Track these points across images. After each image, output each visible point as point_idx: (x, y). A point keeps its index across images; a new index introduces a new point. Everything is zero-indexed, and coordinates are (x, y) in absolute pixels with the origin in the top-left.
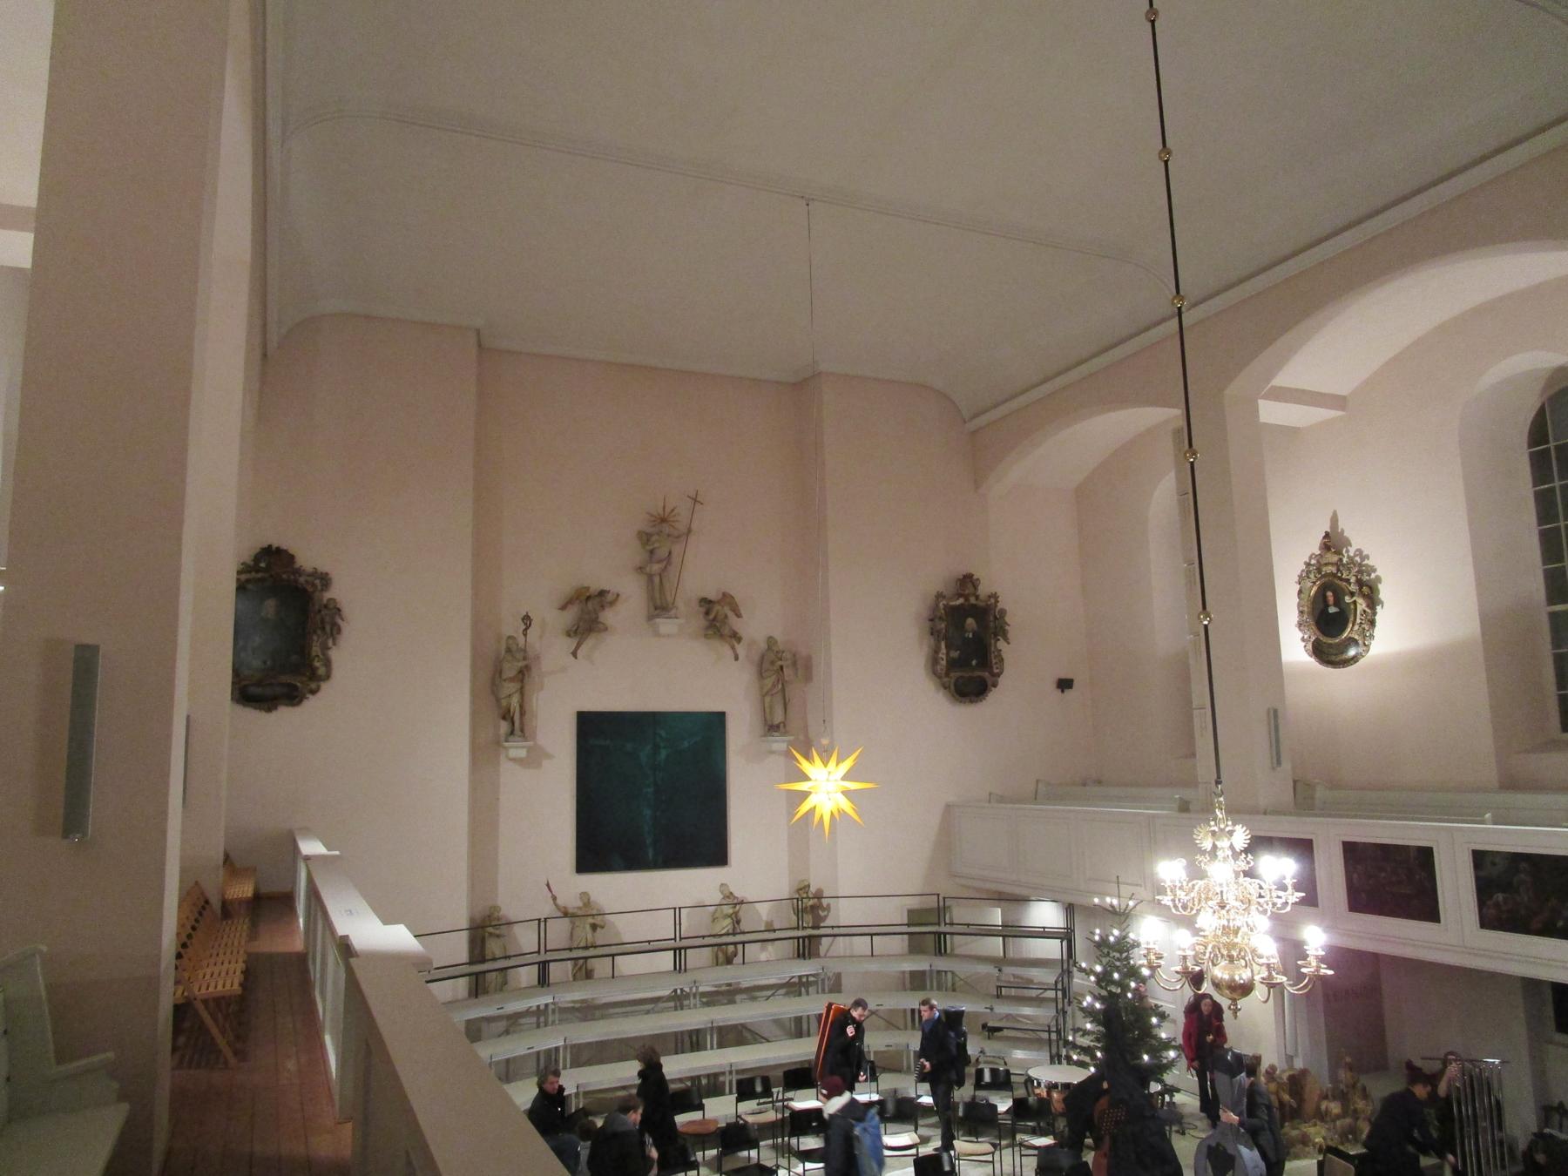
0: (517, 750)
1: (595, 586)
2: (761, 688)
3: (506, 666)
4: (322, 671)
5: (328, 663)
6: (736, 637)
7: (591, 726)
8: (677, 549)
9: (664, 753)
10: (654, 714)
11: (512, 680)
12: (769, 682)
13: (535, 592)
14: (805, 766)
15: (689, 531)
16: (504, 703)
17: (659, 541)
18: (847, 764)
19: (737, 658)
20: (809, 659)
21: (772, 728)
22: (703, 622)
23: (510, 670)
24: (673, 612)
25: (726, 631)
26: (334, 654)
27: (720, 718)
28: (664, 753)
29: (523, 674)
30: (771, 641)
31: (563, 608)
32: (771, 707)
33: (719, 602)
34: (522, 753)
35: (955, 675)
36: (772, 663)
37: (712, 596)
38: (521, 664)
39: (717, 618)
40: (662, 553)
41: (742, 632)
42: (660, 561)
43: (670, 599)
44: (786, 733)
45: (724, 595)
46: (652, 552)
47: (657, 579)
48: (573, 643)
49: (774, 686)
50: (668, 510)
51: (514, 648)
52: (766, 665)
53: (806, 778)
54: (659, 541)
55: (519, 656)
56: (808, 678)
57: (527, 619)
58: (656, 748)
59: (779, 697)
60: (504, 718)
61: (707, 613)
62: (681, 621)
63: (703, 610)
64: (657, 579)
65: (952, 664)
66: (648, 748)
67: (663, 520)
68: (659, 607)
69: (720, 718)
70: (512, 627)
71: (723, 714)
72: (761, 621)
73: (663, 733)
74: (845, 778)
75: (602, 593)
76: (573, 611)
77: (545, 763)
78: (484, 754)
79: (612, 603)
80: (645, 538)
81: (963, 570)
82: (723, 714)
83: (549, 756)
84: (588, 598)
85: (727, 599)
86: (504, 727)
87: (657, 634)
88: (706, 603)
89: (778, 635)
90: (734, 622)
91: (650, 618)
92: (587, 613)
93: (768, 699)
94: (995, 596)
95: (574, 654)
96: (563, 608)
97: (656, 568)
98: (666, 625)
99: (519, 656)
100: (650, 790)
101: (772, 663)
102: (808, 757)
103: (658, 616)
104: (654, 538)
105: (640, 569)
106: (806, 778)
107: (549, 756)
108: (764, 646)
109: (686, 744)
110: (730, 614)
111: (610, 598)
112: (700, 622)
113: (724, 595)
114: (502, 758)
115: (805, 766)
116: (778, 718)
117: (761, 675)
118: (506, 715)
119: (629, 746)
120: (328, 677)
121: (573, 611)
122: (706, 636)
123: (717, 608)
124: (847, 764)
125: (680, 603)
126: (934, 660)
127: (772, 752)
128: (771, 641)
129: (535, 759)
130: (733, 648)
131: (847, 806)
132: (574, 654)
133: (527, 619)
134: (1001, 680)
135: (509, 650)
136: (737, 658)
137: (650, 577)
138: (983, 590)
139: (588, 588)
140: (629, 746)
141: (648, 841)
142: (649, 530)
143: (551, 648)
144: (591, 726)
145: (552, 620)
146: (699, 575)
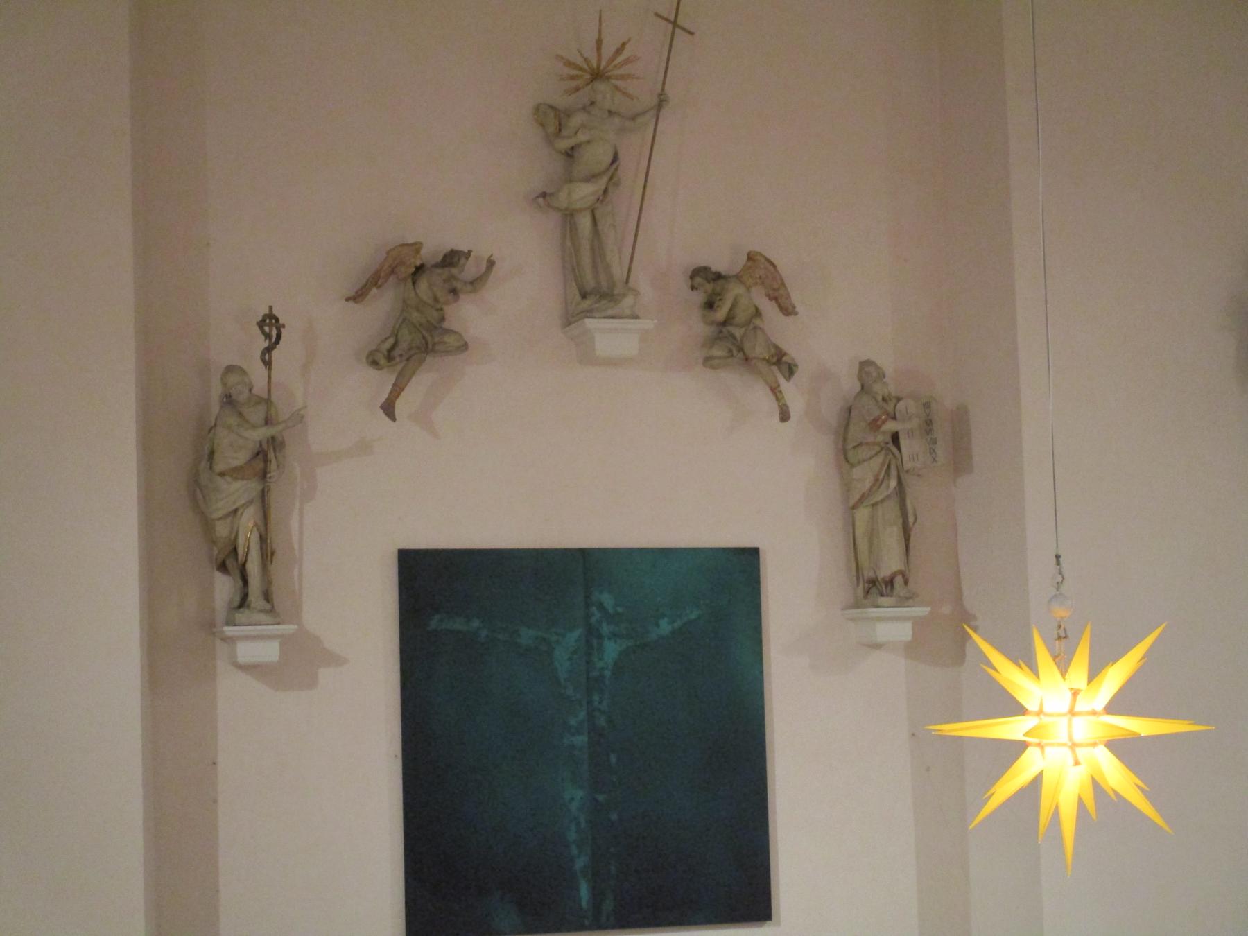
0: (258, 645)
2: (847, 487)
3: (224, 438)
6: (782, 363)
7: (434, 587)
9: (611, 650)
11: (236, 473)
12: (864, 475)
13: (286, 257)
14: (1011, 676)
15: (662, 101)
16: (222, 530)
17: (585, 129)
18: (1116, 676)
19: (785, 416)
20: (960, 418)
21: (874, 587)
22: (699, 327)
23: (235, 449)
24: (628, 301)
25: (758, 350)
27: (748, 559)
28: (611, 650)
29: (264, 460)
31: (358, 296)
32: (872, 534)
33: (738, 277)
34: (268, 652)
36: (875, 425)
37: (719, 266)
38: (261, 434)
39: (733, 316)
40: (597, 155)
41: (794, 352)
42: (591, 178)
43: (618, 272)
44: (908, 600)
45: (751, 257)
46: (570, 154)
47: (585, 222)
48: (383, 381)
49: (878, 482)
50: (608, 51)
51: (243, 397)
52: (857, 431)
53: (1015, 708)
54: (585, 129)
55: (256, 415)
56: (961, 461)
57: (271, 325)
58: (592, 633)
59: (890, 511)
60: (223, 567)
61: (710, 305)
62: (647, 324)
63: (699, 297)
64: (585, 222)
67: (597, 75)
68: (592, 290)
69: (748, 559)
70: (235, 343)
71: (754, 553)
72: (841, 324)
73: (607, 599)
74: (1114, 707)
75: (452, 259)
76: (383, 304)
77: (326, 675)
78: (176, 661)
79: (476, 283)
80: (551, 119)
82: (754, 553)
83: (336, 660)
84: (420, 269)
85: (759, 268)
86: (224, 587)
87: (587, 357)
88: (708, 281)
89: (886, 362)
91: (570, 319)
92: (417, 308)
93: (863, 514)
95: (389, 409)
96: (358, 296)
97: (584, 193)
98: (611, 336)
99: (256, 414)
100: (581, 740)
101: (875, 425)
102: (1026, 659)
103: (589, 313)
104: (577, 120)
105: (545, 196)
106: (1015, 708)
107: (336, 660)
108: (849, 384)
109: (665, 627)
110: (769, 309)
111: (470, 269)
113: (751, 257)
114: (222, 666)
115: (1011, 676)
116: (891, 563)
117: (845, 455)
118: (229, 561)
119: (527, 636)
121: (383, 304)
122: (708, 361)
123: (735, 290)
124: (1116, 676)
125: (642, 280)
127: (877, 646)
129: (302, 663)
130: (775, 390)
131: (1117, 777)
132: (389, 409)
133: (271, 325)
135: (229, 400)
136: (785, 416)
137: (569, 216)
139: (416, 247)
140: (527, 636)
141: (580, 863)
142: (562, 101)
143: (331, 394)
144: (434, 587)
146: (684, 213)
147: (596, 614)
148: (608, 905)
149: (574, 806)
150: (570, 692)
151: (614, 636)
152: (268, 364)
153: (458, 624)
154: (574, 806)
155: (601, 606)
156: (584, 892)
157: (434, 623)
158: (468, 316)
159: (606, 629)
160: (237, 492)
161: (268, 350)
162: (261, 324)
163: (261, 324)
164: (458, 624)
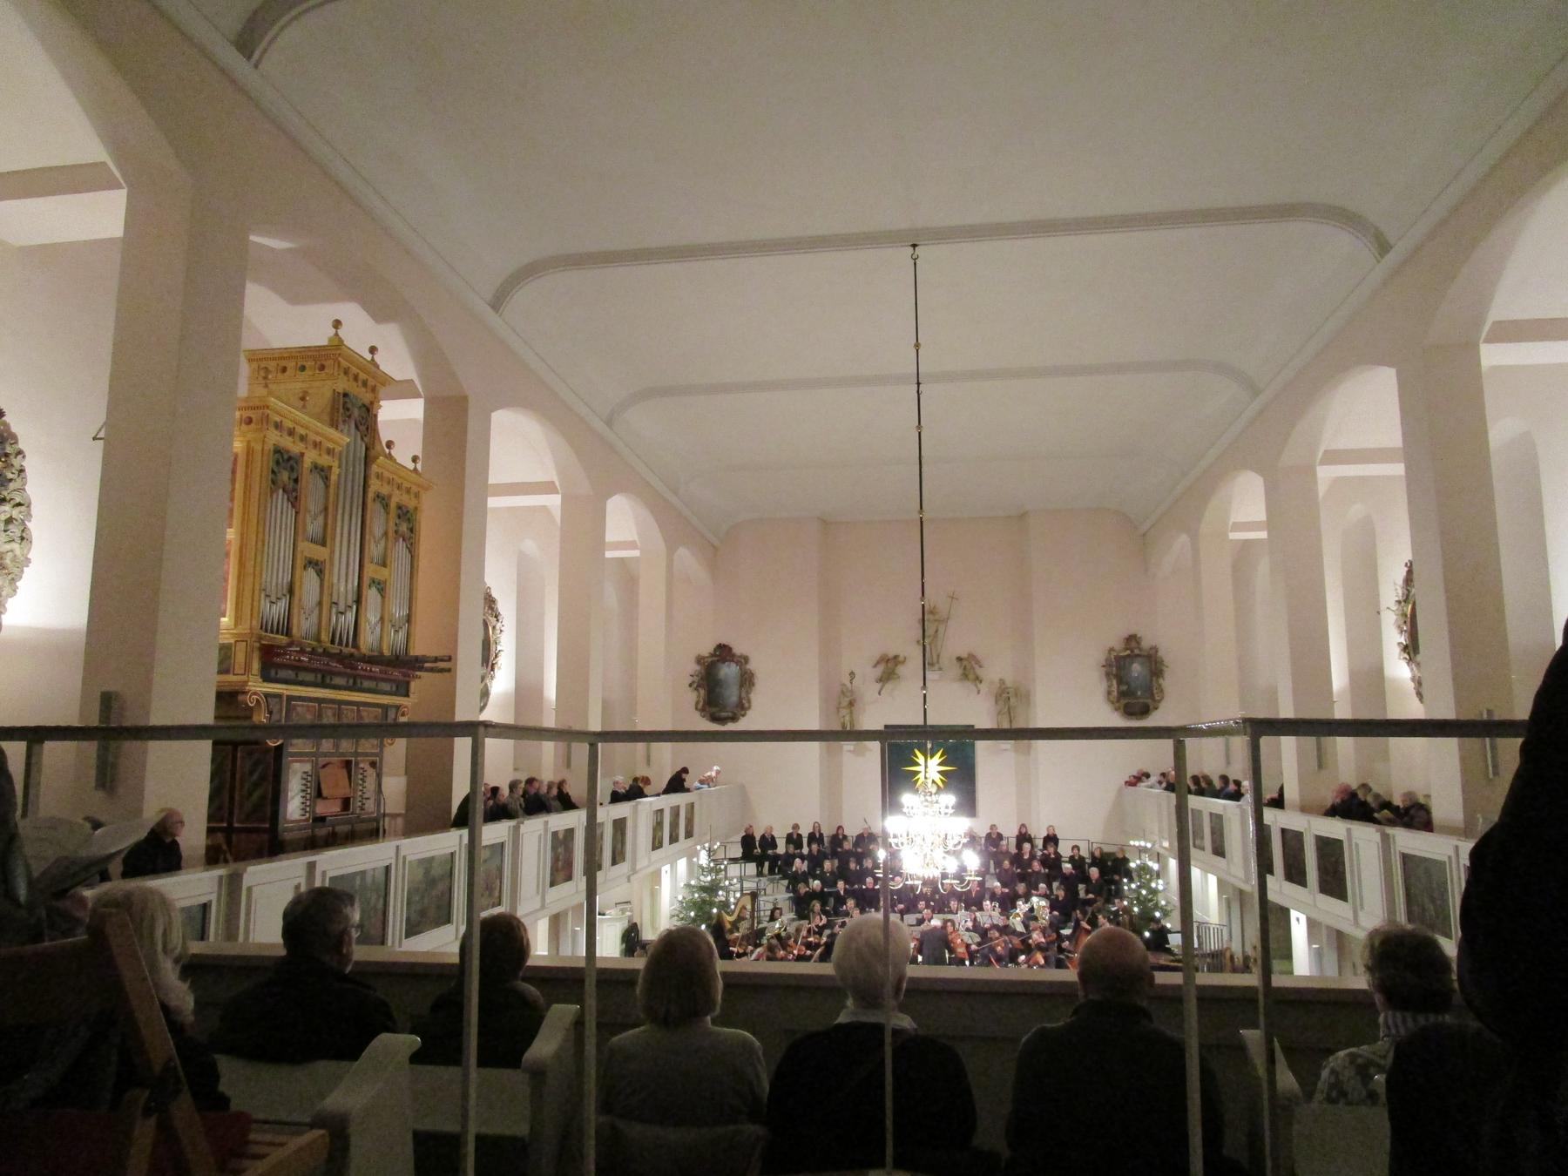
1: (891, 654)
5: (749, 701)
6: (978, 679)
8: (941, 630)
13: (859, 660)
22: (960, 671)
23: (845, 702)
26: (752, 696)
29: (851, 704)
30: (1002, 681)
35: (1124, 702)
37: (964, 655)
39: (968, 668)
48: (879, 686)
57: (852, 674)
65: (1122, 694)
72: (997, 669)
75: (896, 657)
81: (1132, 632)
85: (972, 657)
88: (959, 659)
90: (979, 671)
92: (889, 668)
94: (1155, 649)
112: (957, 670)
121: (881, 668)
125: (944, 661)
126: (1109, 693)
128: (1002, 681)
133: (852, 674)
134: (1163, 705)
138: (1146, 644)
143: (867, 687)
145: (867, 674)
158: (901, 670)
160: (844, 712)
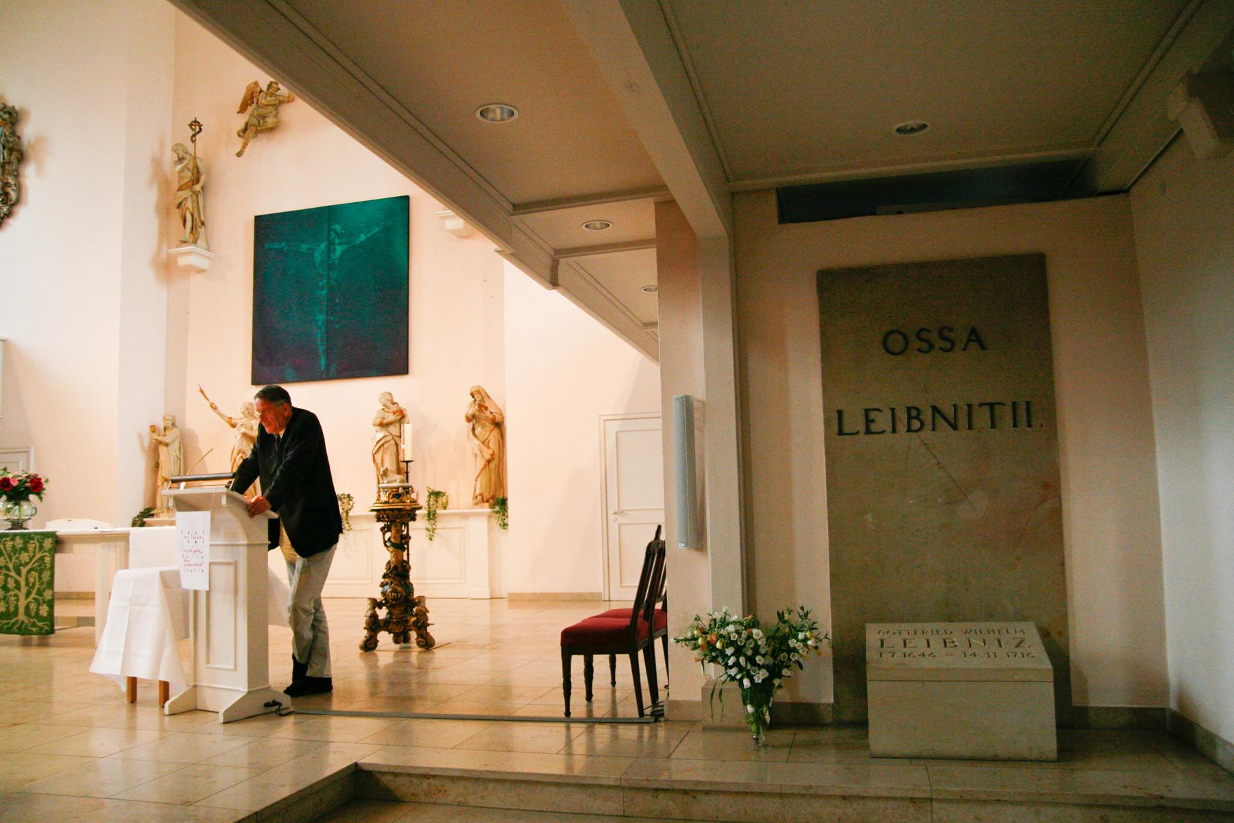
4: (13, 195)
7: (269, 230)
9: (339, 250)
10: (329, 207)
28: (339, 250)
48: (240, 141)
58: (331, 244)
66: (323, 246)
73: (338, 228)
96: (242, 110)
100: (324, 292)
109: (363, 237)
119: (304, 248)
120: (18, 200)
140: (304, 248)
141: (321, 349)
144: (269, 230)
147: (333, 235)
148: (333, 369)
149: (320, 323)
150: (320, 271)
151: (340, 244)
152: (194, 141)
153: (276, 246)
154: (320, 323)
155: (336, 232)
156: (323, 361)
157: (267, 246)
159: (337, 241)
161: (194, 135)
162: (190, 126)
163: (190, 126)
164: (276, 246)
